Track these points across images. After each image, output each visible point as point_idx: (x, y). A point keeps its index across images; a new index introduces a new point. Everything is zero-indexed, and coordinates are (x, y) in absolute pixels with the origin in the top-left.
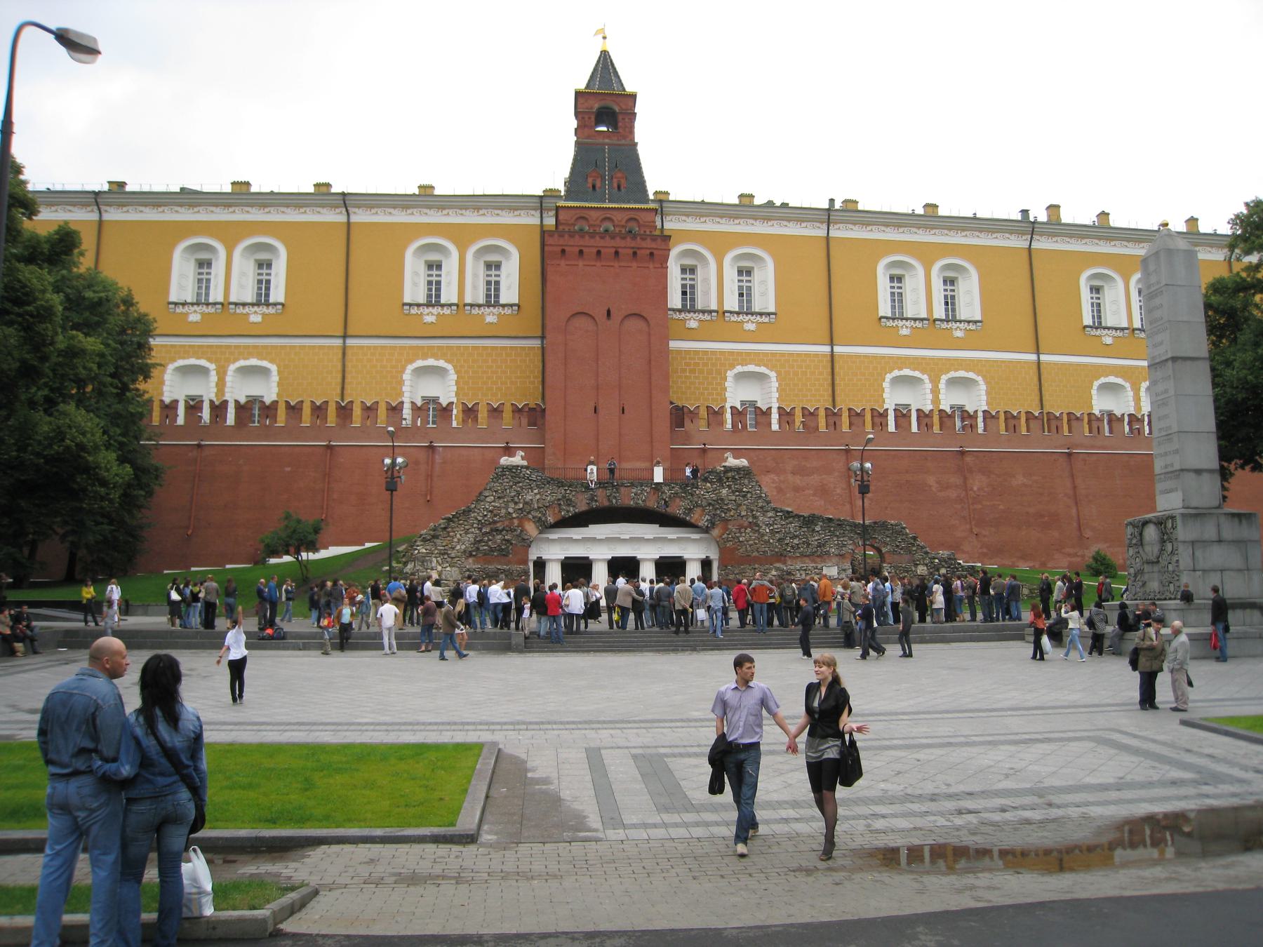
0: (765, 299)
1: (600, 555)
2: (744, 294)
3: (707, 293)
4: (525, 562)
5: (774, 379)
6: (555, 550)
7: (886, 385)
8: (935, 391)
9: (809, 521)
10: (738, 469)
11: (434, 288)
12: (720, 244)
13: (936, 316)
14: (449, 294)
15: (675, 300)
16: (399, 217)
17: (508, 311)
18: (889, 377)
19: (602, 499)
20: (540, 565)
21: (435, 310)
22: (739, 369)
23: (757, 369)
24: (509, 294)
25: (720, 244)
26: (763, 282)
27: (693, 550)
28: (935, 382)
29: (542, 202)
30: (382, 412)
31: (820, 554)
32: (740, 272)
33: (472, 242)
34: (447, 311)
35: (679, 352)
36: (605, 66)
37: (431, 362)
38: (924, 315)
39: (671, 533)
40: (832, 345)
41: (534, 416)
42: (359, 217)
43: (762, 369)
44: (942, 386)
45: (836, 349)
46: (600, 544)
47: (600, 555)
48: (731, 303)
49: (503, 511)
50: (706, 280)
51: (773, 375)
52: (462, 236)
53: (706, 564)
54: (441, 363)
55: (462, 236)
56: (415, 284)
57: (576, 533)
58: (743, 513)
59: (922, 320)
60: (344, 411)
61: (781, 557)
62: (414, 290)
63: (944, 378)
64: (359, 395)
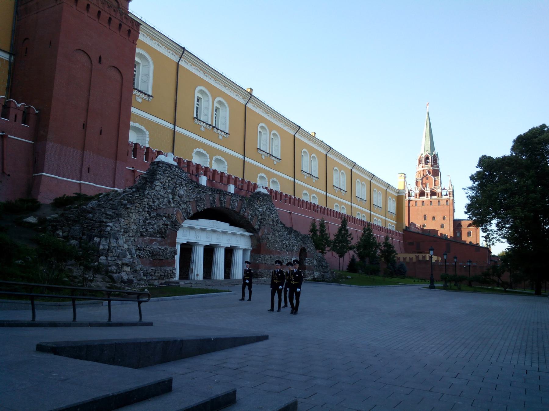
5: (148, 136)
7: (193, 155)
8: (211, 163)
13: (214, 125)
18: (195, 150)
23: (140, 127)
26: (147, 75)
28: (211, 159)
38: (210, 123)
40: (175, 125)
43: (143, 128)
44: (213, 162)
45: (177, 128)
49: (166, 200)
51: (147, 133)
58: (271, 223)
59: (210, 125)
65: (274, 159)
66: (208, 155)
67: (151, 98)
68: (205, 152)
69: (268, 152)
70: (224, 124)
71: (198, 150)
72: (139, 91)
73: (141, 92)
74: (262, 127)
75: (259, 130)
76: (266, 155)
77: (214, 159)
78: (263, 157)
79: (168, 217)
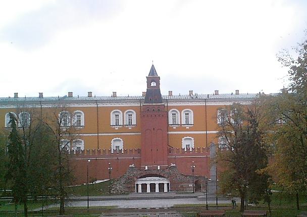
0: (191, 121)
1: (148, 183)
2: (187, 119)
3: (178, 121)
4: (134, 184)
6: (140, 182)
9: (186, 176)
10: (173, 167)
11: (117, 121)
12: (180, 109)
14: (121, 123)
15: (171, 122)
16: (109, 105)
17: (134, 126)
19: (148, 173)
20: (137, 185)
21: (118, 127)
22: (185, 138)
24: (134, 122)
25: (180, 109)
27: (165, 182)
29: (140, 101)
30: (107, 152)
31: (189, 182)
32: (186, 114)
33: (126, 110)
34: (120, 127)
35: (172, 134)
36: (153, 71)
37: (117, 138)
39: (163, 178)
41: (139, 151)
42: (100, 105)
46: (148, 181)
47: (148, 183)
48: (184, 122)
50: (178, 117)
52: (123, 109)
53: (168, 184)
54: (119, 139)
55: (123, 109)
56: (113, 120)
57: (144, 179)
60: (99, 152)
61: (181, 183)
62: (113, 122)
64: (102, 148)
79: (132, 179)
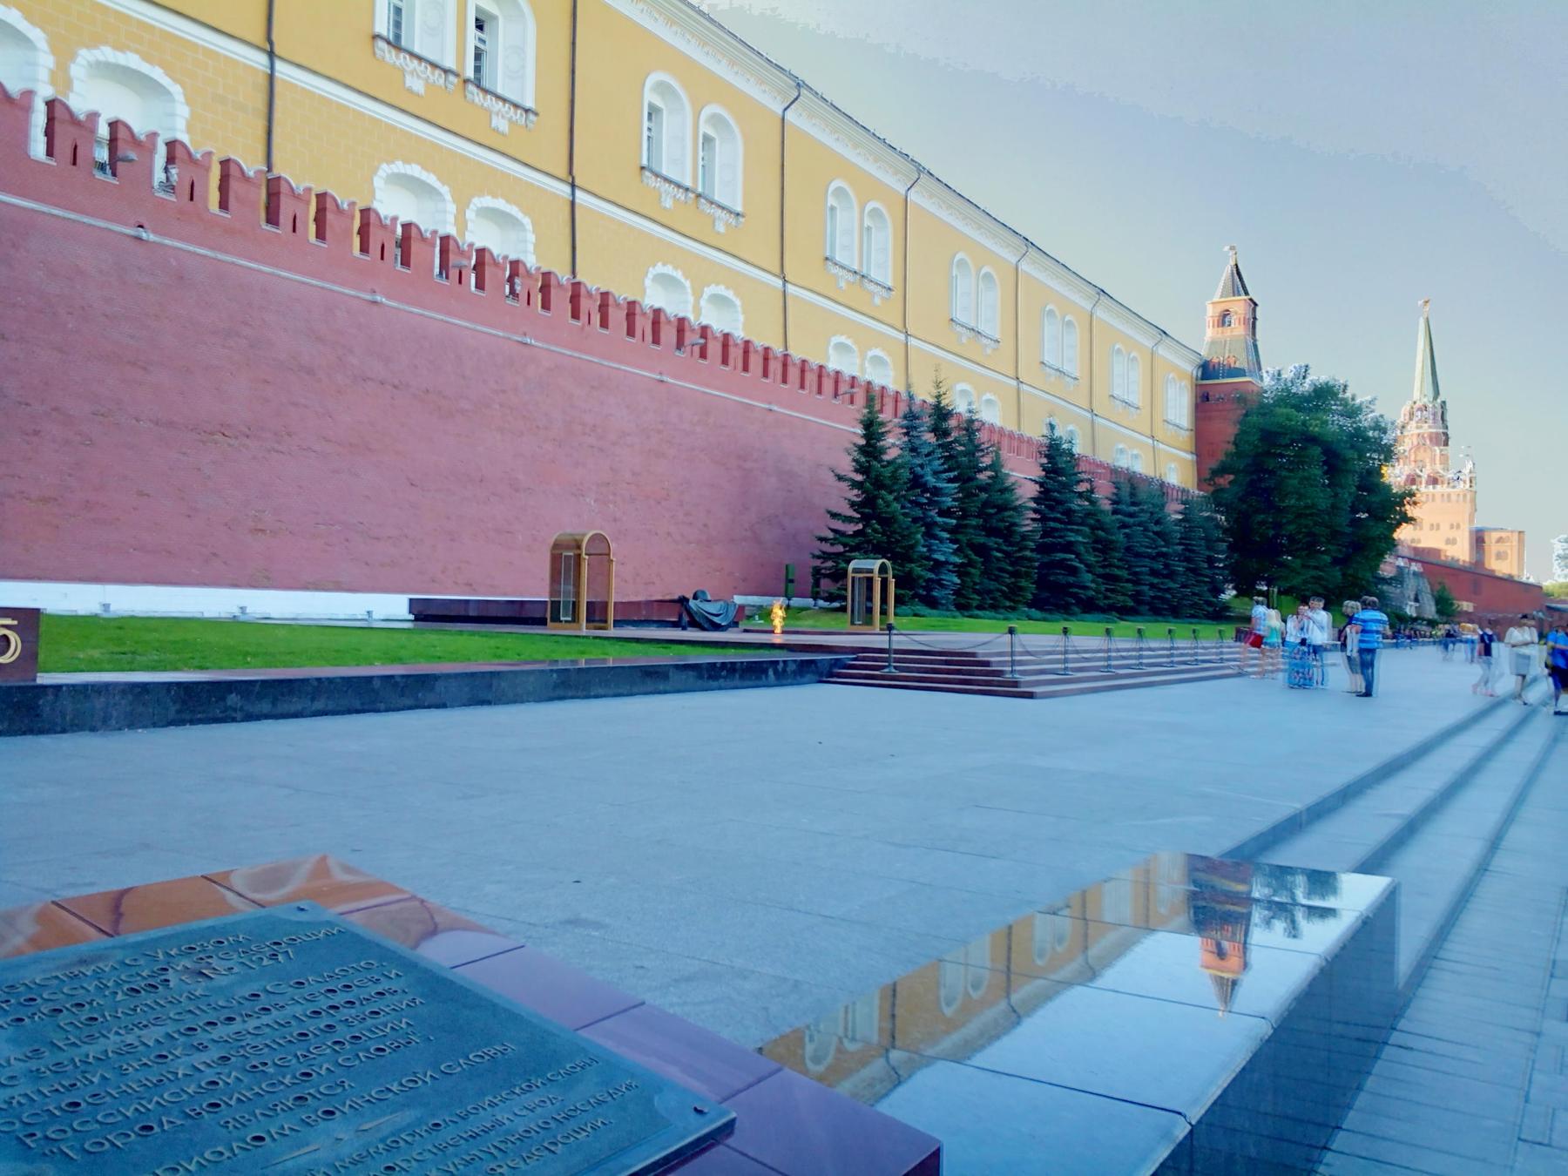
7: (648, 282)
18: (652, 272)
63: (708, 291)
65: (872, 287)
66: (688, 284)
67: (531, 117)
68: (678, 275)
69: (856, 268)
70: (729, 187)
71: (660, 268)
72: (498, 97)
73: (505, 100)
74: (839, 192)
75: (831, 201)
76: (850, 277)
77: (705, 296)
78: (843, 284)
